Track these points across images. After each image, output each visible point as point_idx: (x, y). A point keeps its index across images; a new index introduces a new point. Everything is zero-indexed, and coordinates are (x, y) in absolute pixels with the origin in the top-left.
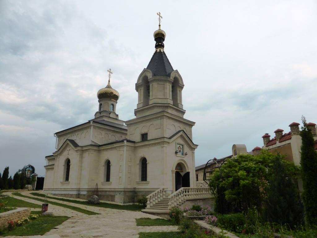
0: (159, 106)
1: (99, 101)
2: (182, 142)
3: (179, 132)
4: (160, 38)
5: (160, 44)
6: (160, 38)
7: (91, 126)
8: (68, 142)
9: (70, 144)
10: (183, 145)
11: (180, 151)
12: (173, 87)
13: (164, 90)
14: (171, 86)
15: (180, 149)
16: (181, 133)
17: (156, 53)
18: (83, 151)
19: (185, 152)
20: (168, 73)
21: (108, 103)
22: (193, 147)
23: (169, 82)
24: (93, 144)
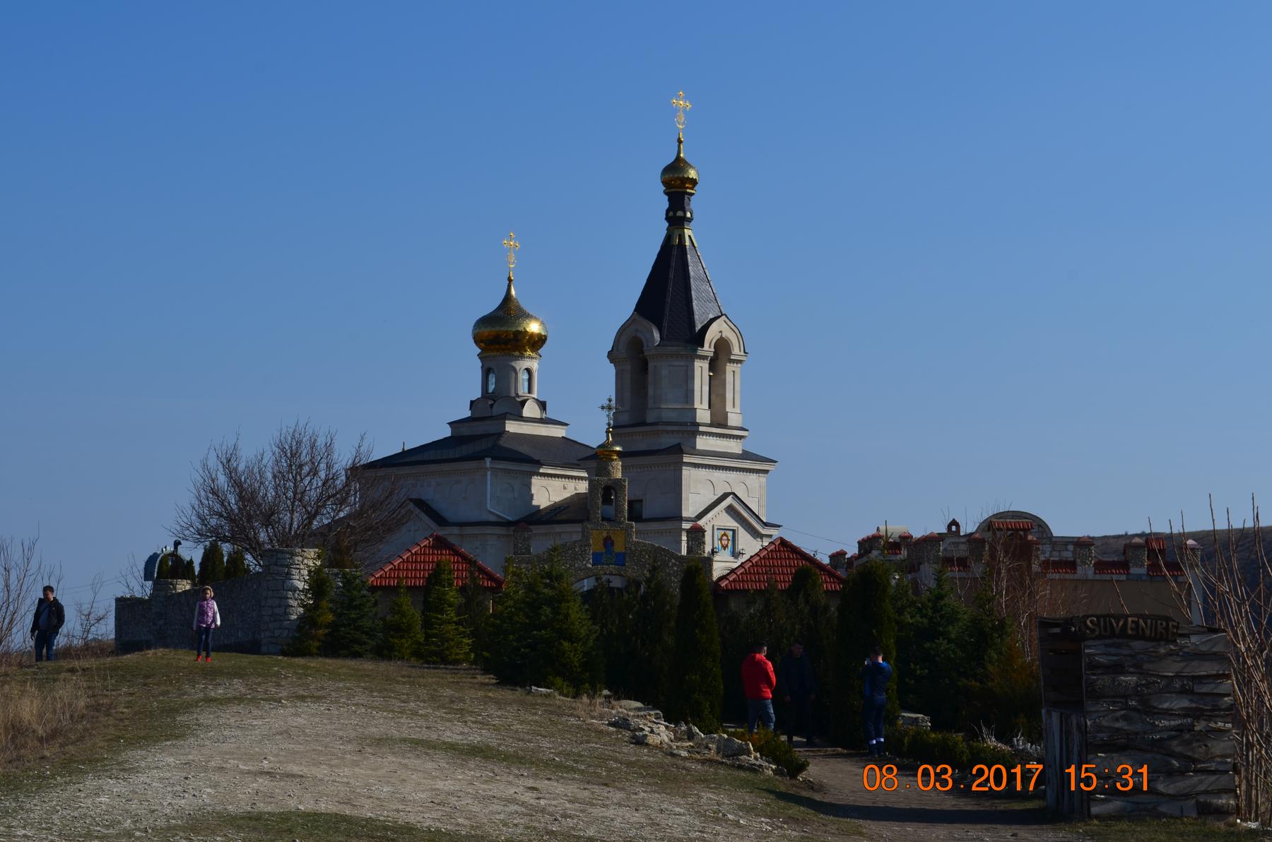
0: (673, 432)
1: (480, 356)
2: (733, 524)
3: (725, 496)
4: (677, 186)
5: (680, 213)
6: (677, 186)
7: (487, 469)
8: (411, 506)
9: (417, 511)
10: (734, 531)
11: (725, 547)
12: (711, 369)
13: (687, 382)
14: (705, 365)
15: (725, 542)
16: (729, 500)
17: (668, 238)
18: (462, 536)
19: (740, 547)
20: (698, 327)
21: (515, 370)
22: (764, 531)
23: (703, 358)
24: (492, 519)
